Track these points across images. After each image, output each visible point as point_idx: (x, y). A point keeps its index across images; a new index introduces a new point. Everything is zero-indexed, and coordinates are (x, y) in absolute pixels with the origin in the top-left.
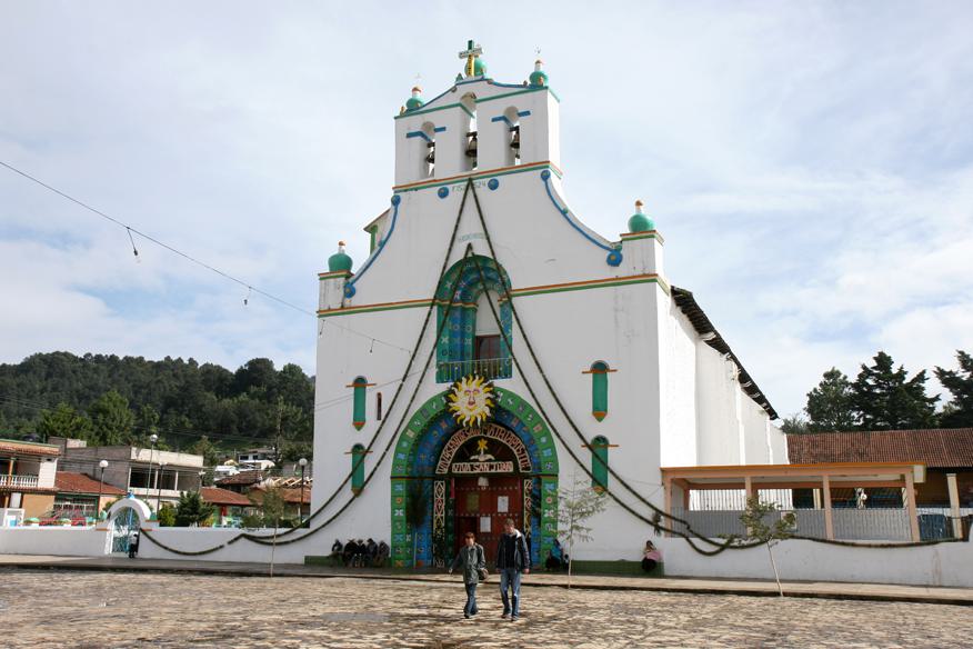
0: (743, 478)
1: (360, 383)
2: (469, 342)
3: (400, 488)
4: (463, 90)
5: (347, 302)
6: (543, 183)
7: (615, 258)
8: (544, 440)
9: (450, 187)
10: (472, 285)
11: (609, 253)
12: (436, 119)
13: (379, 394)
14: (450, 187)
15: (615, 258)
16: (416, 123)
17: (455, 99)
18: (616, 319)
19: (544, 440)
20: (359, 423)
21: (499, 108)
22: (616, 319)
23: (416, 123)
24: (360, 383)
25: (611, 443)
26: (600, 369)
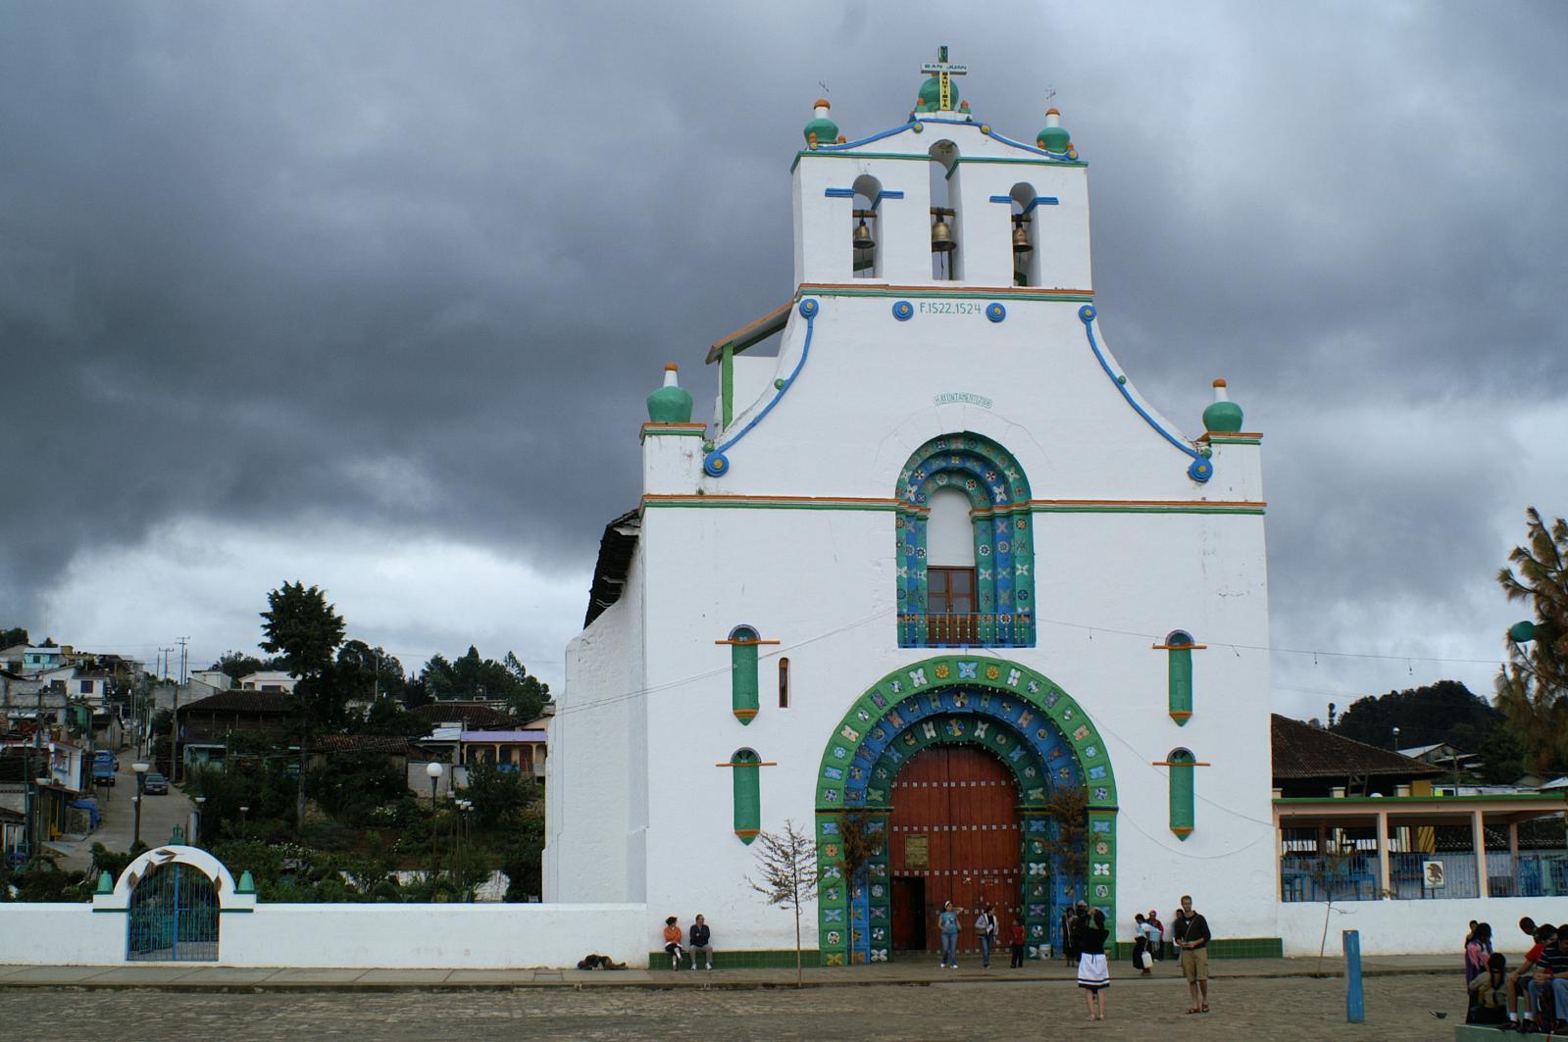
0: (1378, 814)
1: (744, 640)
2: (923, 575)
3: (831, 828)
4: (933, 134)
5: (713, 486)
6: (1083, 326)
7: (1200, 474)
8: (1091, 752)
9: (915, 302)
10: (933, 475)
11: (1193, 460)
12: (887, 176)
13: (784, 662)
14: (915, 302)
15: (1200, 474)
16: (844, 172)
17: (921, 144)
18: (1203, 565)
19: (1091, 752)
20: (746, 710)
21: (1005, 180)
22: (1203, 565)
23: (844, 172)
24: (744, 640)
25: (1198, 761)
26: (1180, 644)
